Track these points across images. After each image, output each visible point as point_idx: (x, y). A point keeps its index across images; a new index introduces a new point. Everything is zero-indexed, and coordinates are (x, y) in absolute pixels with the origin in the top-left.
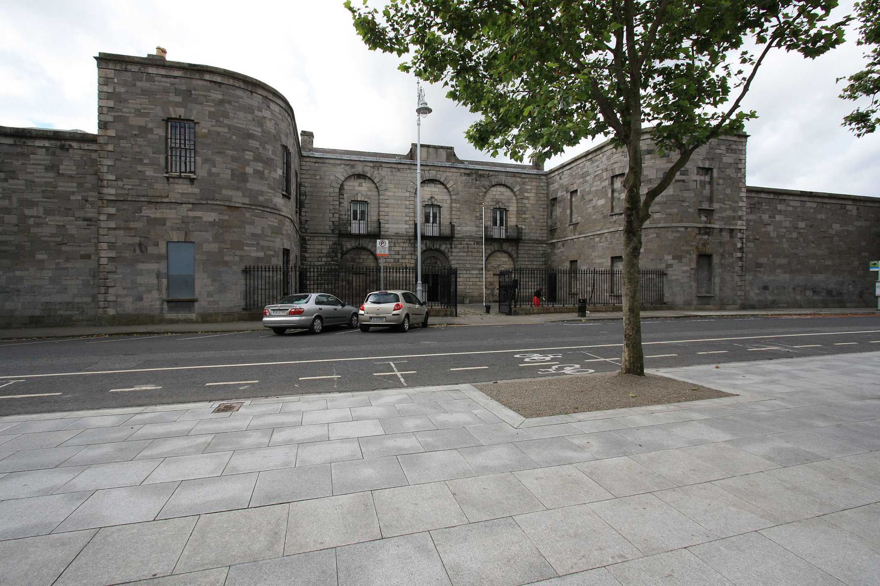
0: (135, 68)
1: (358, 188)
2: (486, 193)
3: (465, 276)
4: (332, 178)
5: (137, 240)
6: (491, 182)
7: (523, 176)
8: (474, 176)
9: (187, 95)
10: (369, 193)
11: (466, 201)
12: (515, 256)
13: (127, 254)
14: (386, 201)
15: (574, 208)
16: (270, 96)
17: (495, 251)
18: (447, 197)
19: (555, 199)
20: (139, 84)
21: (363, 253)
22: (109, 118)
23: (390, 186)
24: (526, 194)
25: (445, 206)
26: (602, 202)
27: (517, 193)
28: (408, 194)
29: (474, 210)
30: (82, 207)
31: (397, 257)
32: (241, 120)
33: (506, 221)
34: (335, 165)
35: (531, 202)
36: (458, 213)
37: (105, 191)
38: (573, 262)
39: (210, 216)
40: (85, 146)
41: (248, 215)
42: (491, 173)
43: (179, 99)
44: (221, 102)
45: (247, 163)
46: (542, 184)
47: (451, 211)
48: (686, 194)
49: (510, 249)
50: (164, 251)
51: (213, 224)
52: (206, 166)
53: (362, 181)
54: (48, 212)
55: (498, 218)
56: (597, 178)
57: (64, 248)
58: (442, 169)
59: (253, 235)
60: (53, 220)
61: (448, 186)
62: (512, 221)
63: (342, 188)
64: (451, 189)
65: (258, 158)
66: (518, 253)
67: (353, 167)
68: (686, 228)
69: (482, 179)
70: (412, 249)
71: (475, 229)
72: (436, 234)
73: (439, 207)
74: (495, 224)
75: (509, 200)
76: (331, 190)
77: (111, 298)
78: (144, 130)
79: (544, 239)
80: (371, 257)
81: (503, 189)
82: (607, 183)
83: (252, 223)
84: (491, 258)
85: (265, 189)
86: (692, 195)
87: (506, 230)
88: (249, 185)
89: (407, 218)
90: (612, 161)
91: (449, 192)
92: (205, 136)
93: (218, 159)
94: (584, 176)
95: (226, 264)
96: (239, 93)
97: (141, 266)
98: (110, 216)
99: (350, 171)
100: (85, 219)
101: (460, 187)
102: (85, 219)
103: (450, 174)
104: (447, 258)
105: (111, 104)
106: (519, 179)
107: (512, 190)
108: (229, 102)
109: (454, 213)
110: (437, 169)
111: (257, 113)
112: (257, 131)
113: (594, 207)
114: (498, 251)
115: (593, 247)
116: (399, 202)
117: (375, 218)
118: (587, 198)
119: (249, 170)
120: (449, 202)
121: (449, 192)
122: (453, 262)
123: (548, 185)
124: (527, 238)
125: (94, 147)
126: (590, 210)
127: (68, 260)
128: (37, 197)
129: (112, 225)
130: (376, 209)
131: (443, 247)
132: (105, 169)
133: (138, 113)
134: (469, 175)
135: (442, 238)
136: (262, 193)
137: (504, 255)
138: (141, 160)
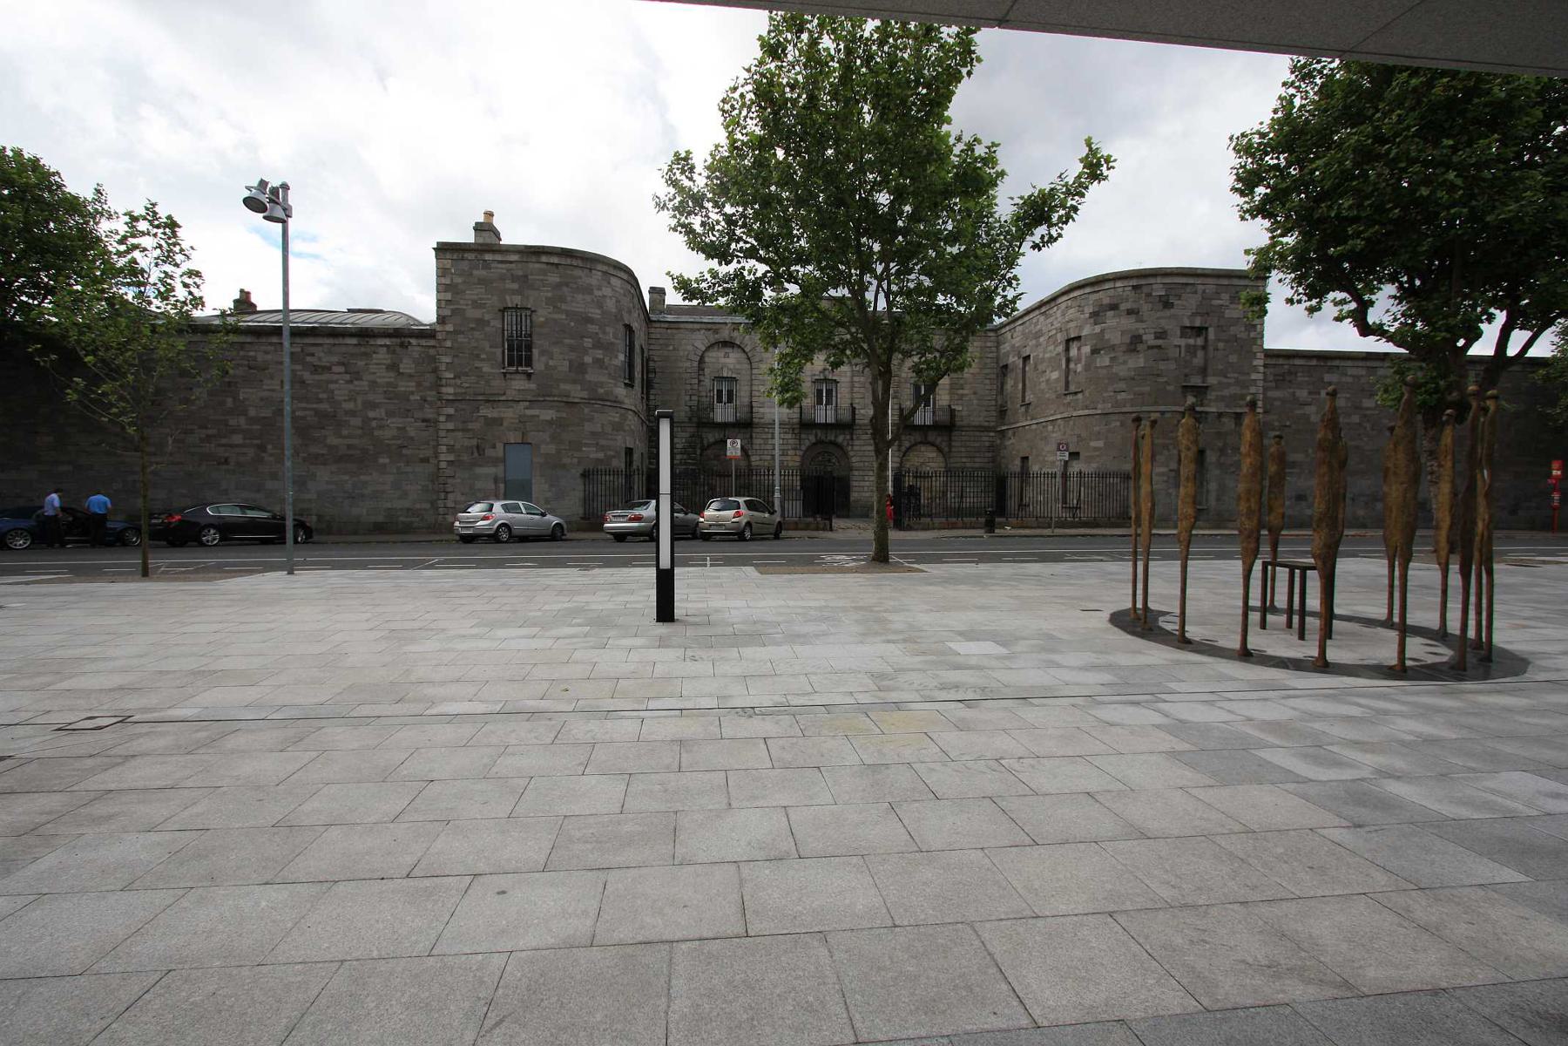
0: (471, 256)
1: (723, 360)
4: (690, 348)
5: (474, 442)
9: (524, 280)
13: (465, 458)
16: (612, 271)
19: (1006, 366)
20: (475, 272)
22: (447, 312)
26: (1055, 375)
30: (421, 408)
32: (579, 304)
34: (693, 330)
37: (444, 390)
38: (1025, 459)
39: (548, 414)
40: (423, 342)
41: (586, 410)
43: (515, 286)
44: (558, 286)
45: (585, 351)
47: (852, 387)
48: (1162, 366)
50: (501, 454)
51: (550, 423)
52: (543, 359)
53: (728, 350)
54: (390, 414)
57: (405, 451)
59: (593, 433)
60: (395, 422)
63: (702, 360)
65: (598, 345)
66: (950, 446)
67: (716, 332)
68: (1163, 413)
76: (688, 364)
77: (450, 504)
78: (481, 323)
82: (1061, 348)
83: (591, 420)
84: (911, 454)
85: (604, 379)
86: (1173, 366)
88: (588, 377)
92: (542, 325)
93: (556, 350)
94: (1038, 335)
95: (564, 466)
96: (578, 272)
97: (479, 470)
98: (449, 417)
99: (713, 338)
100: (424, 421)
102: (424, 421)
104: (845, 454)
105: (449, 296)
108: (567, 285)
111: (597, 293)
112: (595, 313)
117: (746, 400)
119: (588, 359)
123: (998, 344)
124: (965, 423)
125: (432, 342)
126: (1043, 386)
127: (408, 463)
128: (379, 398)
129: (450, 426)
131: (840, 439)
132: (443, 367)
133: (476, 304)
135: (839, 426)
136: (601, 385)
138: (478, 356)
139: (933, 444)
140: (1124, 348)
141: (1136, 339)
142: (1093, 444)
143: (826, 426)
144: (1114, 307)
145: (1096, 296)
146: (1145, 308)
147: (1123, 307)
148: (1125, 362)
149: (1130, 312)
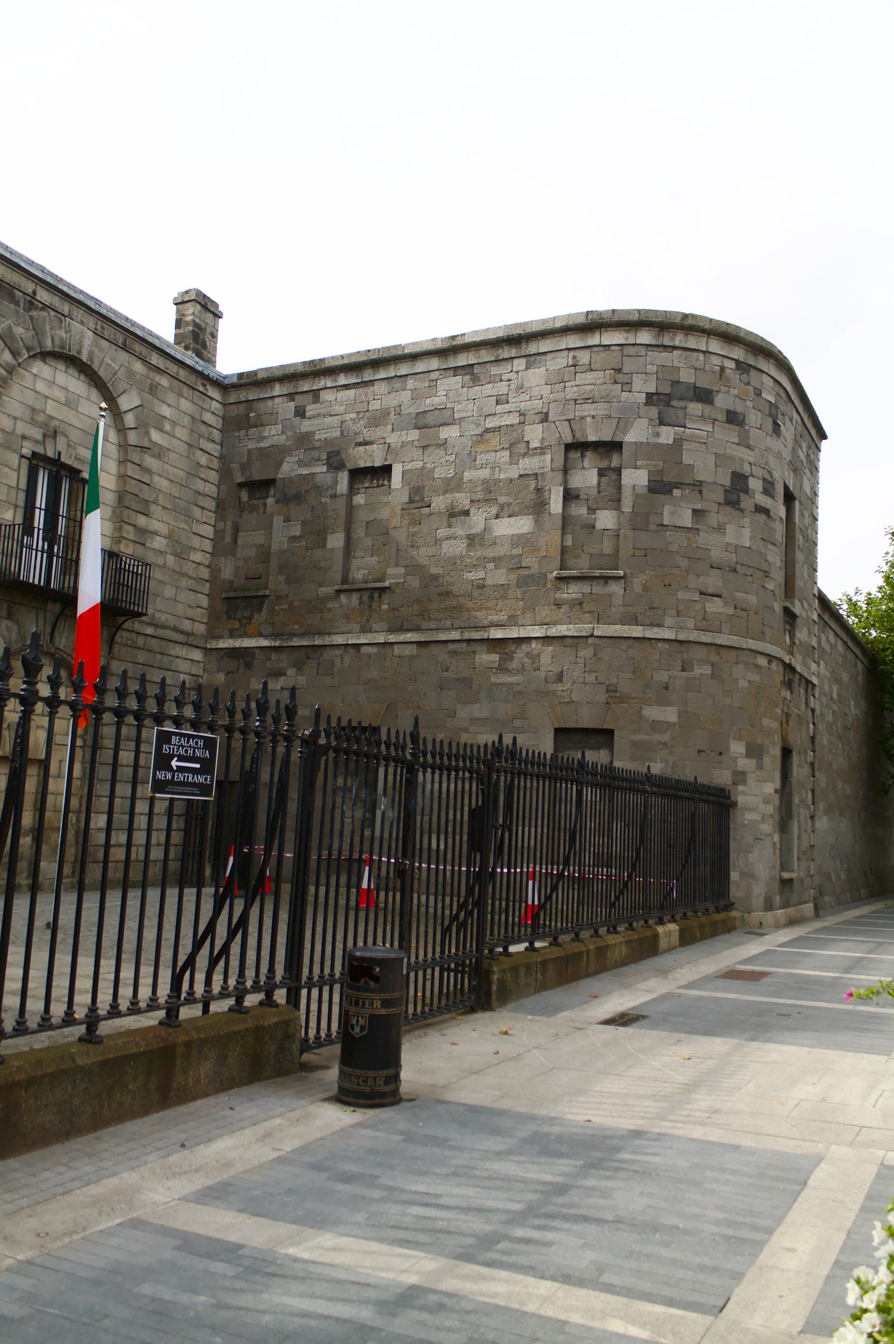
6: (38, 333)
7: (155, 359)
24: (155, 436)
26: (523, 525)
27: (130, 420)
42: (43, 296)
56: (494, 440)
90: (571, 392)
106: (138, 367)
113: (472, 540)
115: (465, 682)
118: (439, 503)
140: (720, 496)
141: (739, 481)
142: (652, 713)
144: (704, 396)
145: (664, 358)
146: (754, 419)
147: (722, 401)
148: (720, 529)
149: (733, 418)
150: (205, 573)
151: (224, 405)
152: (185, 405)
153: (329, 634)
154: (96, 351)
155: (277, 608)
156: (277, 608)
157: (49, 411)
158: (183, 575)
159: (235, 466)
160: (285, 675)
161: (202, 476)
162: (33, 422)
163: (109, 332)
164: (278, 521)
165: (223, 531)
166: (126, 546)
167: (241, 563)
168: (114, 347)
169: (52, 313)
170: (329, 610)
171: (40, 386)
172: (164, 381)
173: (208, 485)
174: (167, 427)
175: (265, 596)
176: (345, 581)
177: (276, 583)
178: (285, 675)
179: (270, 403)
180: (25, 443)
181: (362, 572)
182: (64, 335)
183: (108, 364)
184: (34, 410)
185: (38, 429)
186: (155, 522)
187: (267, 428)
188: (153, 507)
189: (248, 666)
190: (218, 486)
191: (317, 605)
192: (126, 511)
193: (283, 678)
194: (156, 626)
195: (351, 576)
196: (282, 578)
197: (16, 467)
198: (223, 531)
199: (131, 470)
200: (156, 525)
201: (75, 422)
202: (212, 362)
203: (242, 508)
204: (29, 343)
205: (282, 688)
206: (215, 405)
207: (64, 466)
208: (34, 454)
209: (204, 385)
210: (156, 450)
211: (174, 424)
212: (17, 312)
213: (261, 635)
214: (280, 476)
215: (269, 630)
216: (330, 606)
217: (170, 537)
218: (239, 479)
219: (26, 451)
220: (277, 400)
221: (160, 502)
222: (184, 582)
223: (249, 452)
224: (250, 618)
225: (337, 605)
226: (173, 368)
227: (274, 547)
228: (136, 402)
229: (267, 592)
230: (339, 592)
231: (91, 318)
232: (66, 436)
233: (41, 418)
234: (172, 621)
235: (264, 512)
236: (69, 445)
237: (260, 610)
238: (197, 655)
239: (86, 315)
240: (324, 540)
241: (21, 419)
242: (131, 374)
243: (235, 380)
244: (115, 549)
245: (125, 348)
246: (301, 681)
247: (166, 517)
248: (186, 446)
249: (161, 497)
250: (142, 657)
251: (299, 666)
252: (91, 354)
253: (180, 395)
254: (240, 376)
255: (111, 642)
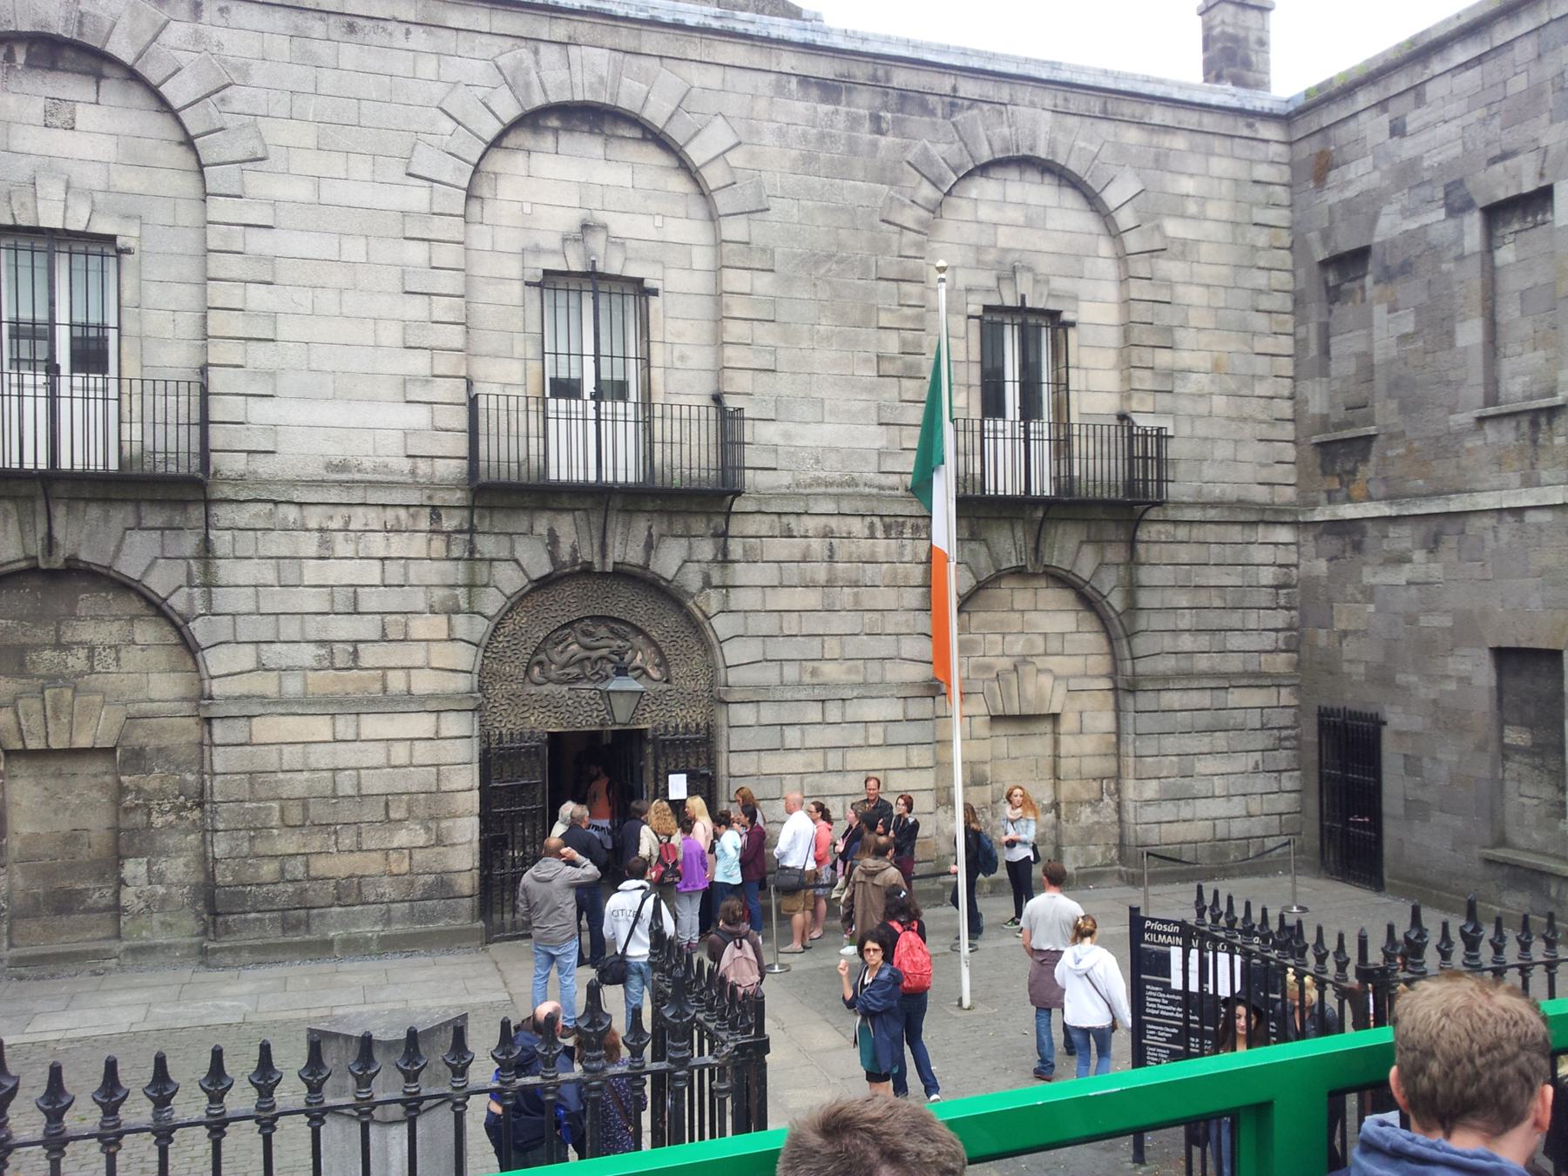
1: (35, 140)
2: (936, 209)
3: (816, 737)
7: (1159, 115)
8: (863, 102)
10: (129, 181)
11: (814, 260)
12: (1116, 601)
14: (258, 242)
15: (1509, 311)
17: (998, 577)
18: (690, 230)
21: (87, 602)
23: (279, 133)
24: (1173, 228)
25: (680, 289)
27: (1125, 219)
28: (417, 198)
29: (867, 317)
31: (343, 628)
33: (1062, 386)
35: (1206, 273)
36: (764, 334)
42: (968, 88)
46: (1262, 172)
49: (1085, 567)
53: (73, 88)
55: (1011, 370)
58: (652, 41)
61: (697, 153)
62: (1095, 387)
64: (714, 177)
66: (1132, 588)
69: (917, 122)
70: (458, 572)
71: (874, 438)
72: (624, 468)
73: (641, 290)
74: (993, 405)
75: (1076, 259)
79: (1289, 494)
80: (147, 632)
81: (1036, 192)
87: (1062, 445)
89: (418, 363)
91: (704, 193)
101: (775, 164)
103: (713, 77)
104: (696, 627)
106: (1132, 136)
107: (1092, 199)
109: (734, 330)
110: (625, 37)
114: (1019, 573)
116: (355, 250)
117: (176, 359)
120: (702, 258)
121: (704, 193)
122: (733, 653)
130: (186, 296)
131: (668, 561)
134: (829, 89)
137: (1052, 596)
139: (1061, 579)
143: (598, 500)
150: (1286, 409)
151: (1290, 144)
152: (1220, 166)
153: (1471, 491)
154: (1060, 137)
155: (1389, 453)
156: (1389, 453)
157: (1003, 242)
158: (1245, 420)
159: (1314, 236)
160: (1410, 561)
161: (1262, 264)
162: (980, 265)
163: (1077, 102)
164: (1379, 312)
165: (1305, 340)
166: (1142, 401)
167: (1336, 385)
168: (1089, 121)
169: (986, 107)
170: (1468, 451)
171: (985, 213)
172: (1179, 142)
173: (1277, 278)
174: (1192, 208)
175: (1370, 438)
176: (1492, 398)
177: (1385, 414)
178: (1410, 561)
179: (1352, 124)
180: (971, 298)
181: (1520, 380)
182: (1006, 130)
183: (1081, 149)
184: (979, 249)
185: (987, 273)
186: (1185, 354)
187: (1353, 165)
188: (1180, 334)
189: (1357, 547)
190: (1293, 272)
191: (1445, 445)
192: (1135, 351)
193: (1408, 566)
194: (1204, 505)
195: (1502, 390)
196: (1393, 405)
197: (962, 334)
198: (1305, 340)
199: (1137, 289)
200: (1185, 359)
201: (1045, 246)
202: (1262, 85)
203: (1334, 295)
204: (955, 161)
205: (1409, 583)
206: (1276, 150)
207: (1033, 311)
208: (987, 309)
209: (1250, 126)
210: (1177, 248)
211: (1203, 200)
212: (934, 124)
213: (1370, 498)
214: (1377, 239)
215: (1382, 490)
216: (1468, 445)
217: (1217, 368)
218: (1321, 254)
219: (975, 309)
220: (1363, 117)
221: (1192, 324)
222: (1248, 430)
223: (1330, 209)
224: (1353, 472)
225: (1480, 443)
226: (1190, 119)
227: (1378, 356)
228: (1134, 187)
229: (1372, 430)
230: (1481, 420)
231: (1046, 93)
232: (1030, 269)
233: (991, 256)
234: (1232, 493)
235: (1363, 300)
236: (1036, 281)
237: (1365, 460)
238: (1284, 534)
239: (1037, 91)
240: (1451, 334)
241: (963, 267)
242: (1121, 150)
243: (1301, 102)
244: (1126, 409)
245: (1106, 117)
246: (1436, 570)
247: (1204, 338)
248: (1229, 227)
249: (1192, 313)
250: (1184, 553)
251: (1433, 545)
252: (1052, 144)
253: (1210, 153)
254: (1307, 94)
255: (1132, 543)
